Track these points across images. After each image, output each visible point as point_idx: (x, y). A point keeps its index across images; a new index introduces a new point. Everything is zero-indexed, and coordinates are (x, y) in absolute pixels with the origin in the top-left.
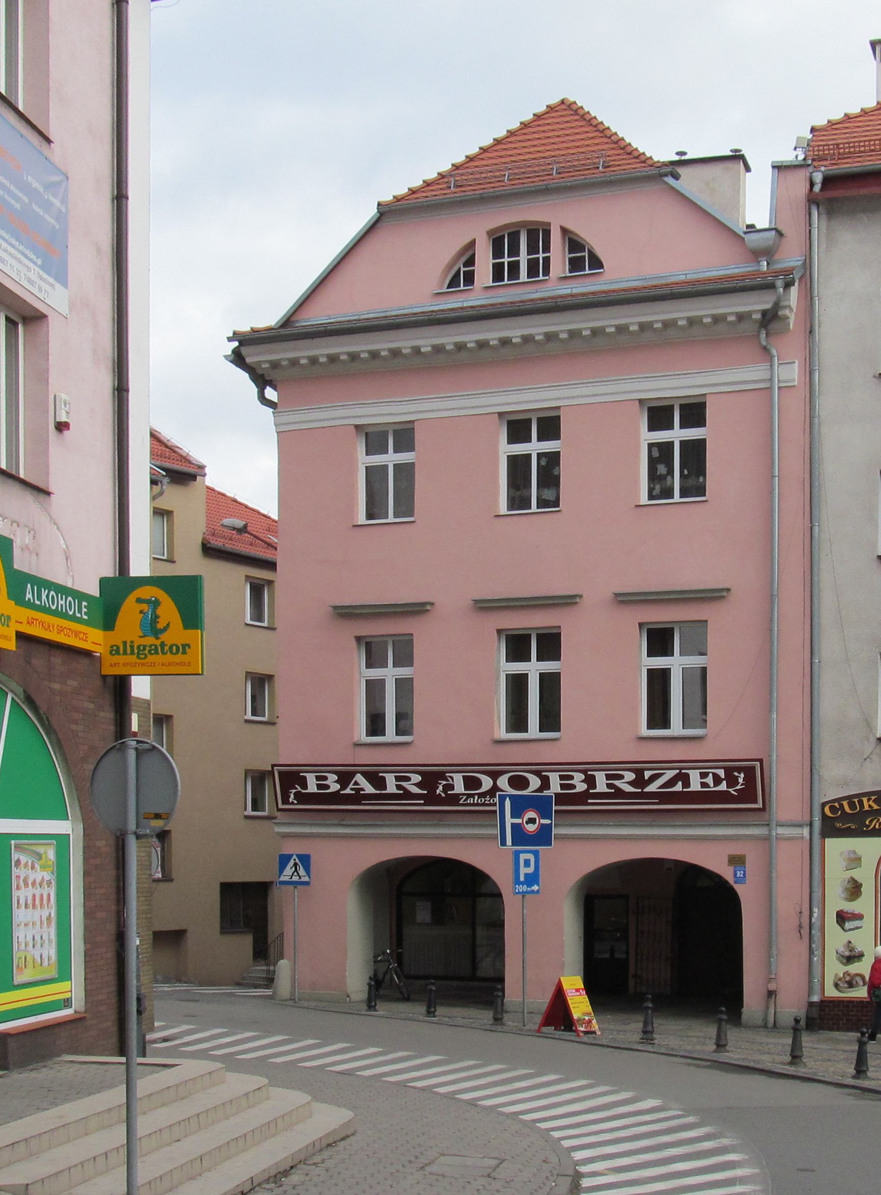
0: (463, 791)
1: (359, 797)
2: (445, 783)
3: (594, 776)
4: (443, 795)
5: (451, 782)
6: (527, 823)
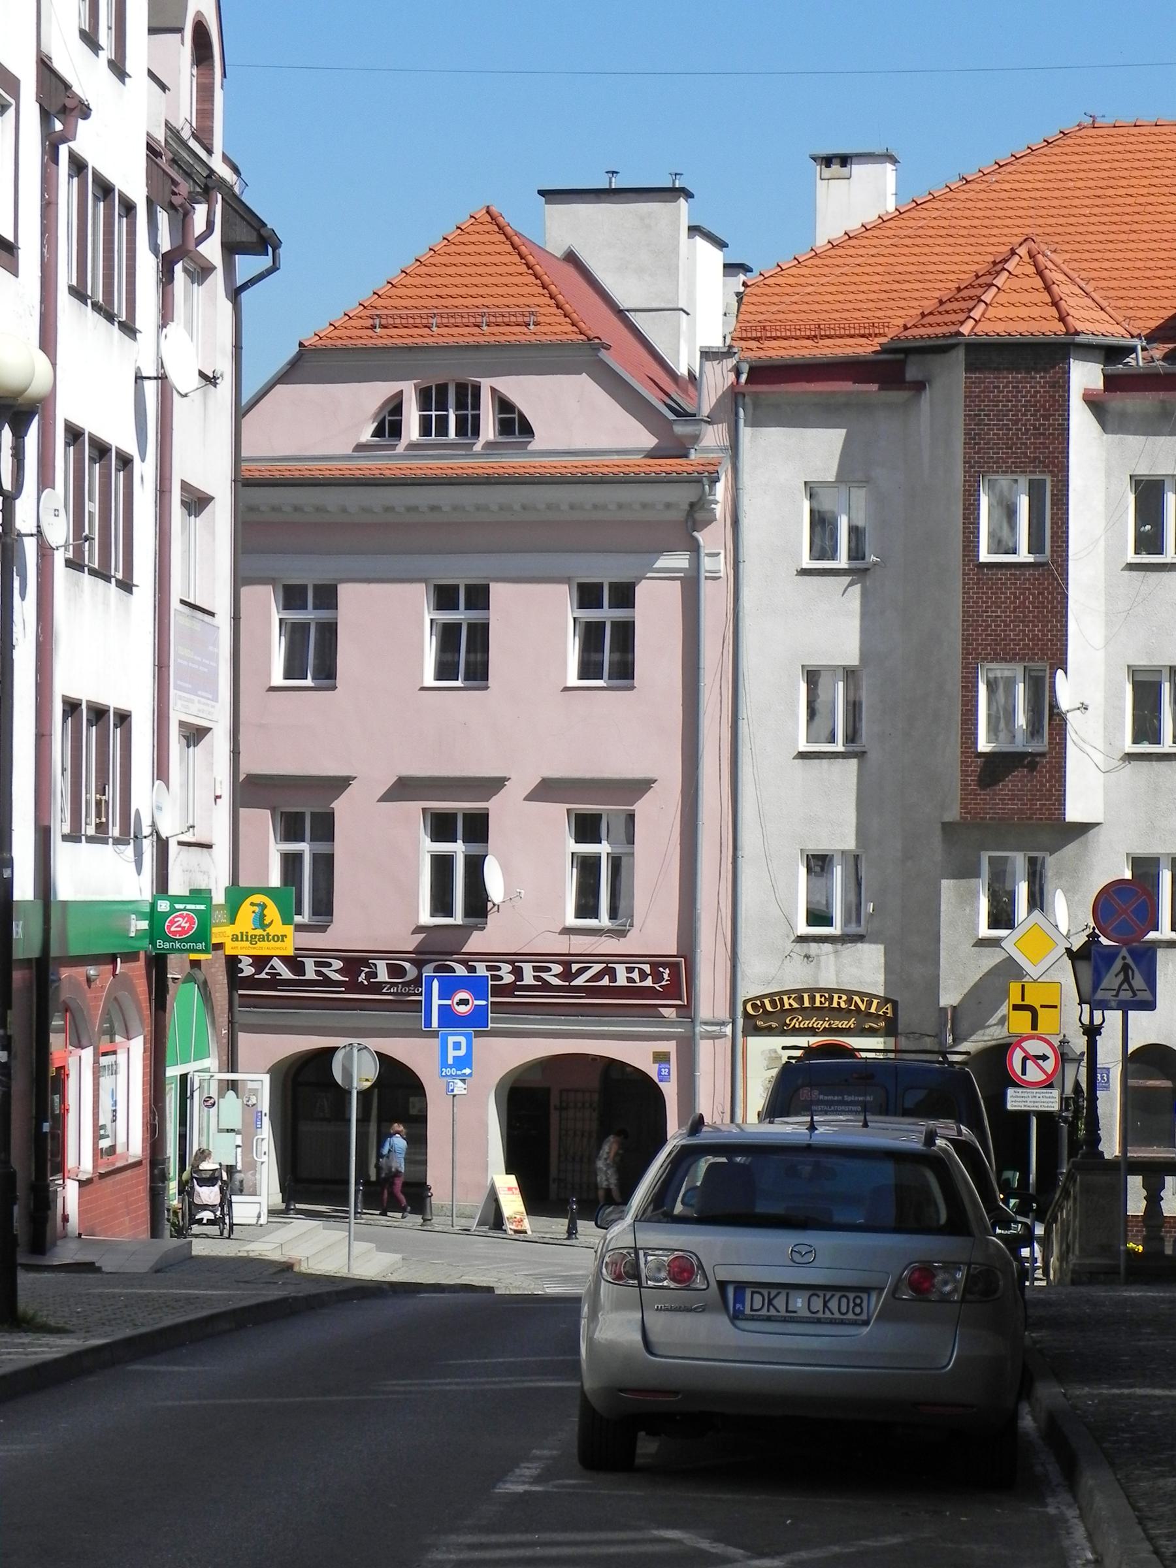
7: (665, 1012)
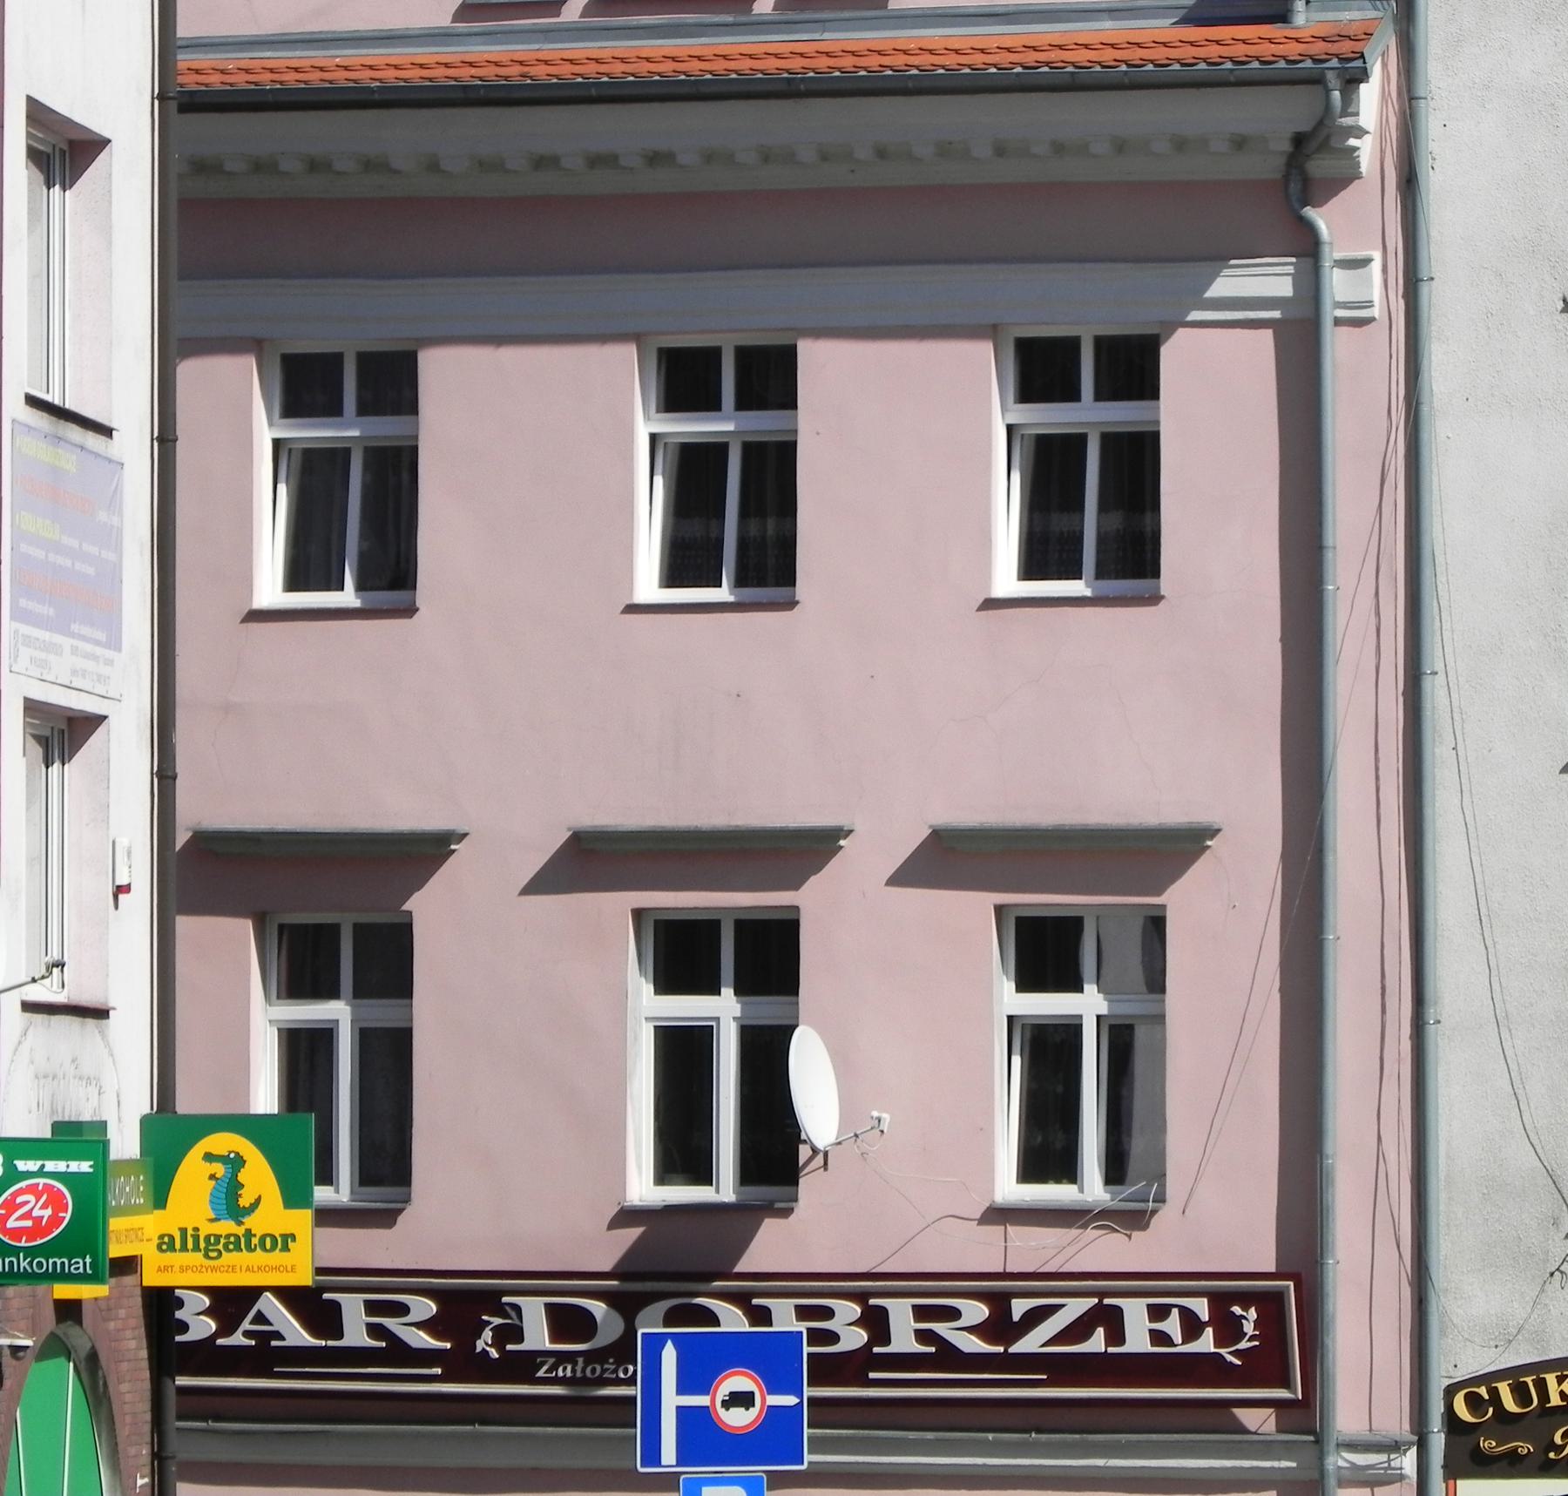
0: (549, 1346)
1: (266, 1355)
2: (497, 1321)
3: (883, 1311)
4: (494, 1354)
5: (517, 1322)
6: (727, 1404)
7: (1251, 1418)
